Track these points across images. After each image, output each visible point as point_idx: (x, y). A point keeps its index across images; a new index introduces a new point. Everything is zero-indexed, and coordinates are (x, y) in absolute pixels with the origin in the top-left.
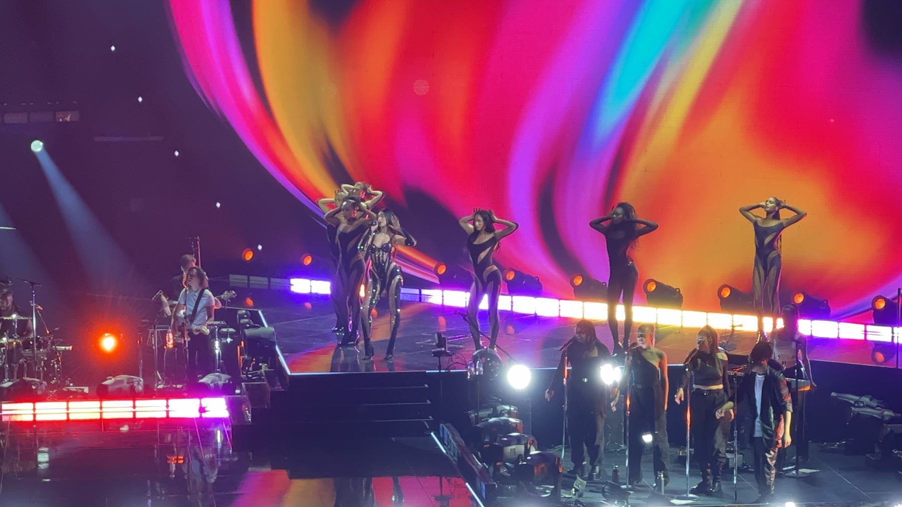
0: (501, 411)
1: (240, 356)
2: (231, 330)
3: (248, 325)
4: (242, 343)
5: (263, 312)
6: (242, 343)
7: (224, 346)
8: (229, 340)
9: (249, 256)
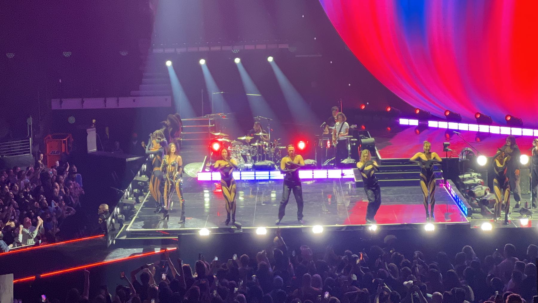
0: (474, 175)
1: (359, 151)
2: (356, 140)
3: (363, 138)
4: (360, 145)
5: (369, 132)
6: (360, 145)
7: (352, 147)
8: (354, 144)
9: (363, 107)
